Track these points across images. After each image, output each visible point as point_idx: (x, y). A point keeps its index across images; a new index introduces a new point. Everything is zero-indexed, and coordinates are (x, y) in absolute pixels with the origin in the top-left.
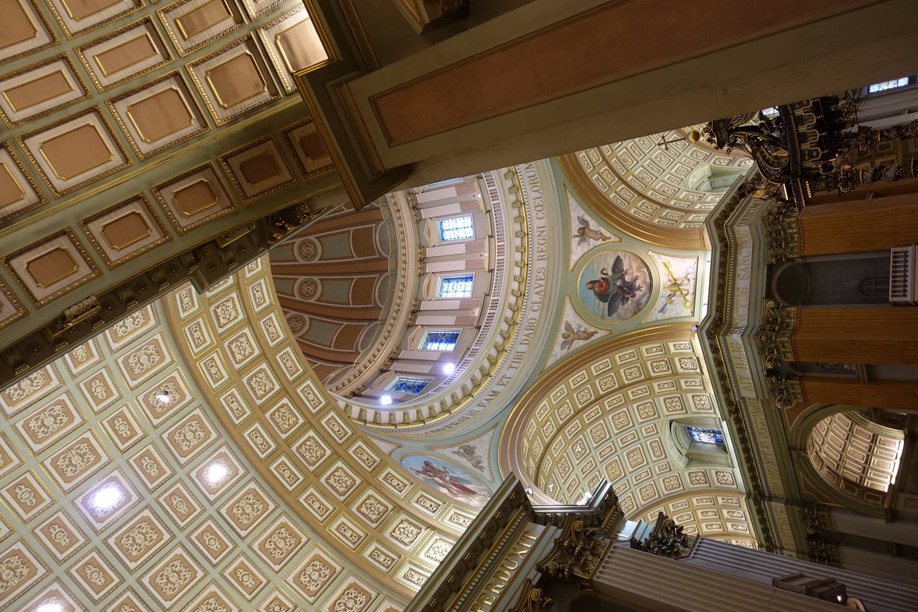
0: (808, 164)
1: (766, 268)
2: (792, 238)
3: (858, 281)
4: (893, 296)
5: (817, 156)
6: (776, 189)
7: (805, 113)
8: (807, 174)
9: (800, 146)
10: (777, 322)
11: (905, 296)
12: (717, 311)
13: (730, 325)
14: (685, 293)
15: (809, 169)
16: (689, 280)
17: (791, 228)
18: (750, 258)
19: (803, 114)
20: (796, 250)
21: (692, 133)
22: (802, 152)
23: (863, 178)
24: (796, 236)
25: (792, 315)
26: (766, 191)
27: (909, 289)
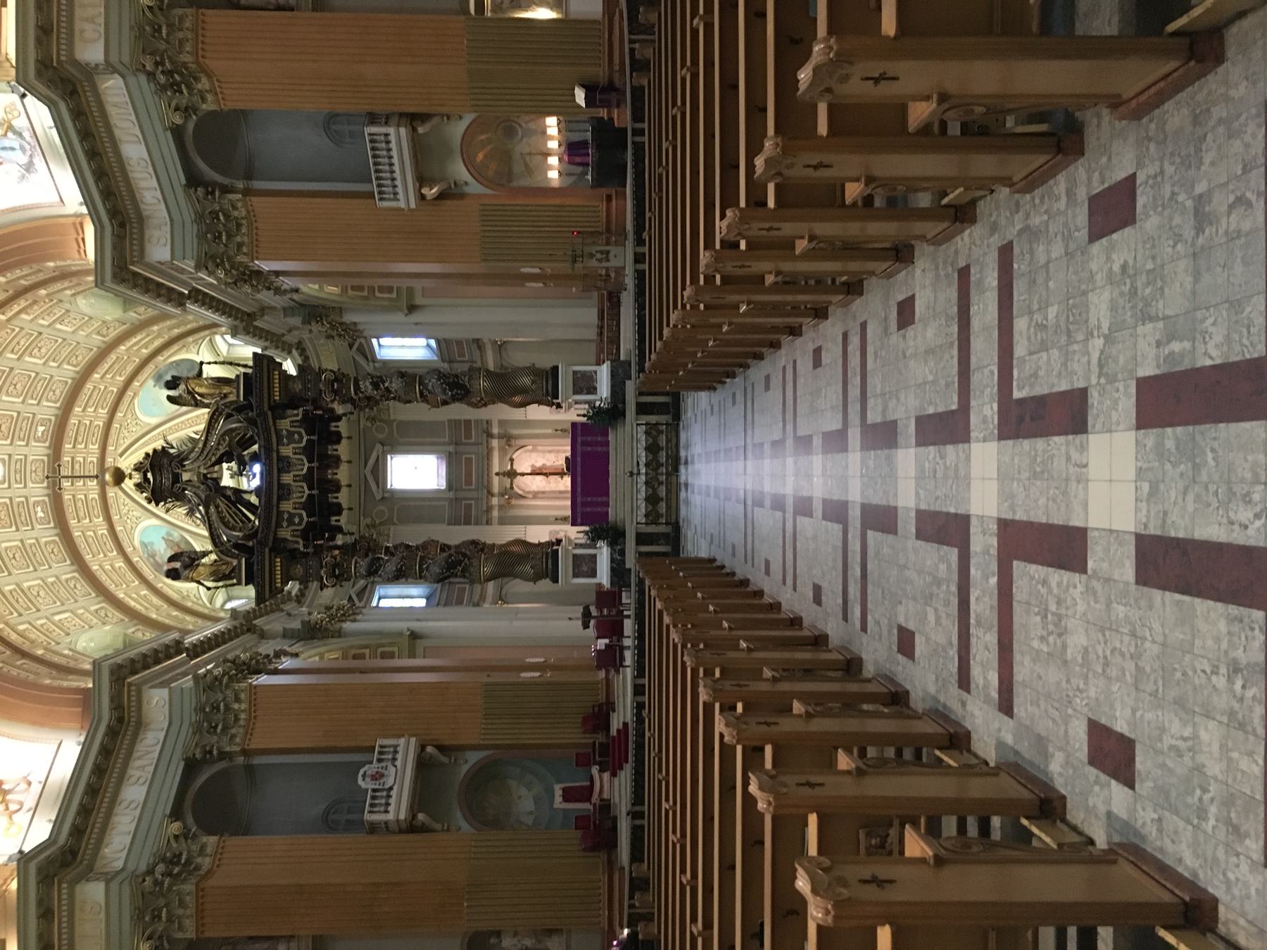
0: (286, 533)
1: (182, 764)
2: (237, 719)
3: (324, 807)
4: (370, 812)
5: (300, 524)
6: (230, 569)
7: (295, 454)
8: (279, 547)
9: (278, 504)
10: (179, 861)
11: (387, 812)
12: (71, 834)
13: (90, 868)
14: (13, 807)
15: (285, 540)
16: (29, 784)
17: (238, 700)
18: (158, 748)
19: (291, 454)
20: (238, 740)
21: (112, 470)
22: (280, 514)
23: (355, 567)
24: (243, 716)
25: (209, 850)
26: (214, 568)
27: (393, 801)
